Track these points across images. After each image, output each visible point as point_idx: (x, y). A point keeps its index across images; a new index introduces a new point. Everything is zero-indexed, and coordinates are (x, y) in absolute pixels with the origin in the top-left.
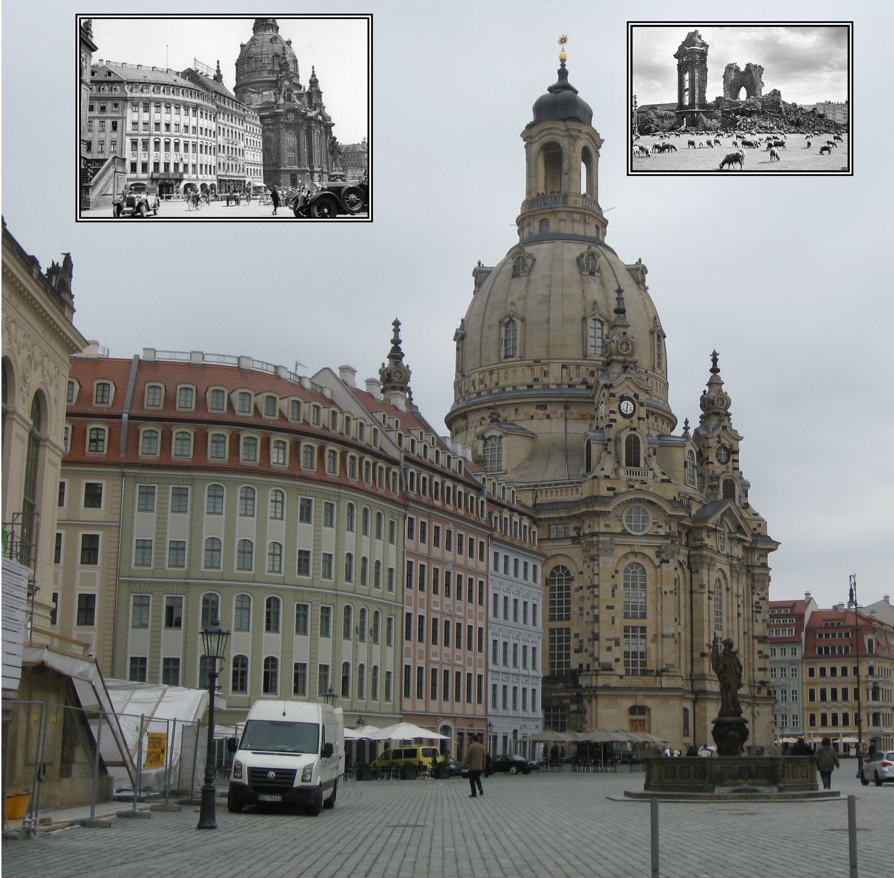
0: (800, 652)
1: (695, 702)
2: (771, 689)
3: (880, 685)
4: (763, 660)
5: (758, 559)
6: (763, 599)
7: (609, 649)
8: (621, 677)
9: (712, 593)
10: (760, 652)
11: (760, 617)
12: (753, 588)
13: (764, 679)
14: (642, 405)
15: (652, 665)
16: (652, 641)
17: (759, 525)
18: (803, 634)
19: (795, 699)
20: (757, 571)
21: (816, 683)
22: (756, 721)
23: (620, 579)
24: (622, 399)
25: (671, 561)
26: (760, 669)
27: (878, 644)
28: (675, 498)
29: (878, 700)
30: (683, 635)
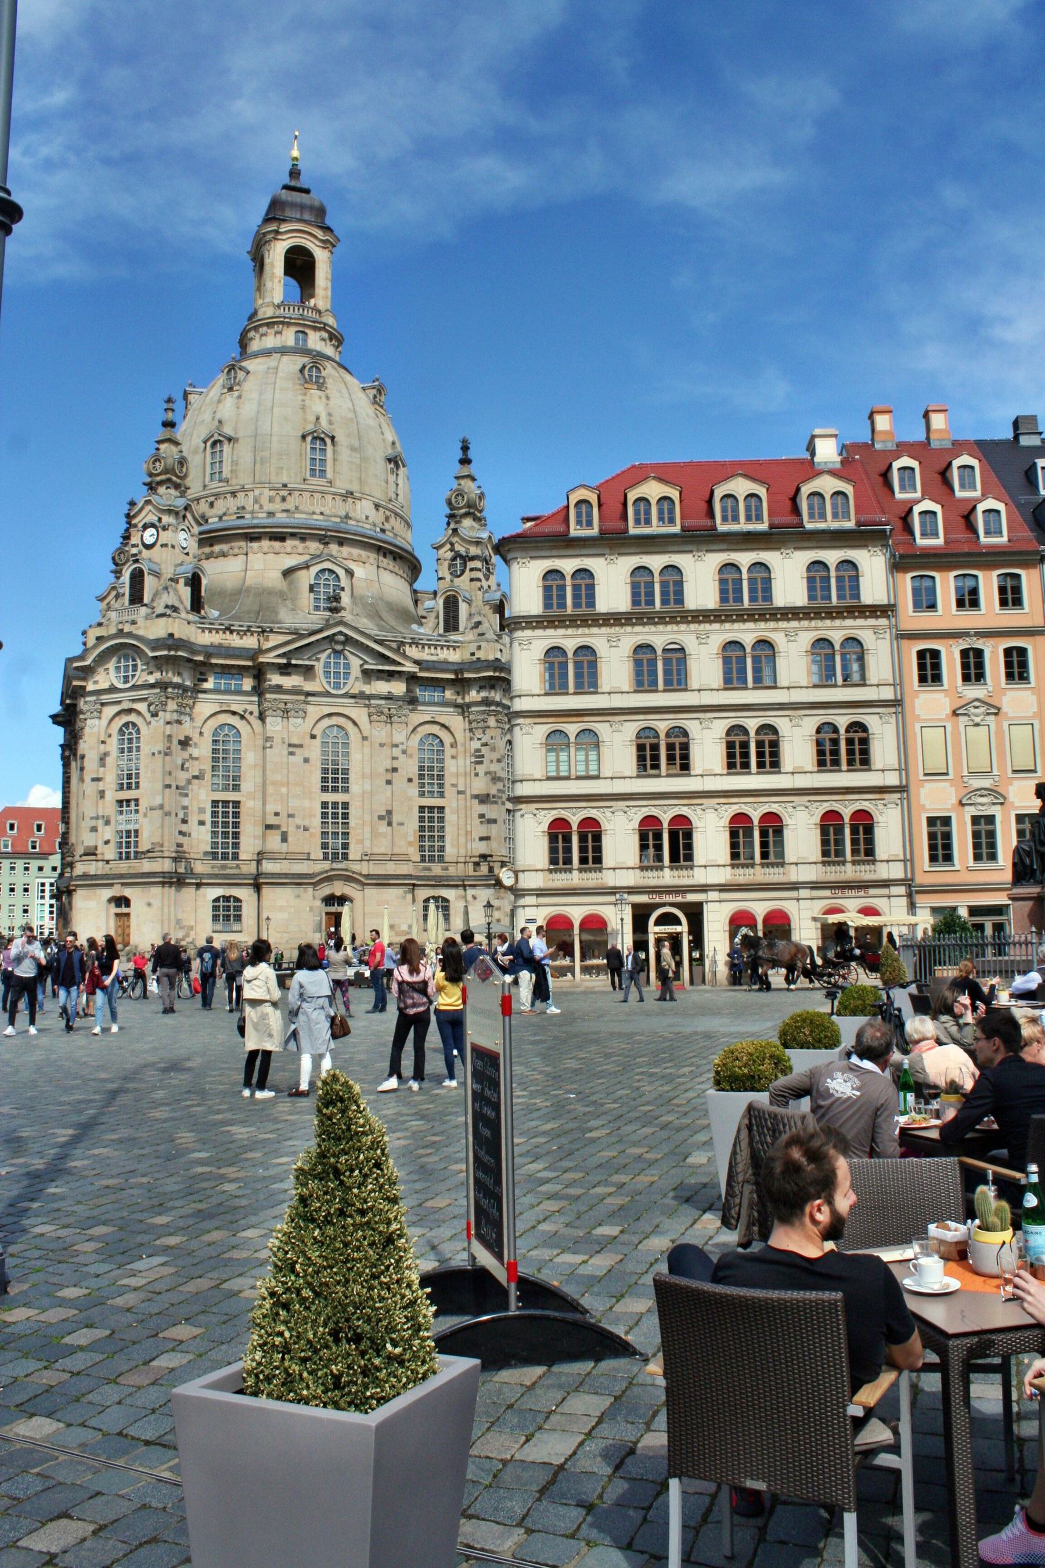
1: (257, 887)
4: (485, 826)
7: (94, 829)
8: (108, 862)
9: (301, 746)
10: (482, 816)
11: (481, 769)
12: (471, 730)
14: (164, 529)
15: (144, 846)
16: (145, 815)
17: (479, 648)
20: (473, 709)
23: (113, 746)
24: (145, 527)
25: (161, 714)
26: (481, 839)
28: (171, 635)
30: (250, 806)
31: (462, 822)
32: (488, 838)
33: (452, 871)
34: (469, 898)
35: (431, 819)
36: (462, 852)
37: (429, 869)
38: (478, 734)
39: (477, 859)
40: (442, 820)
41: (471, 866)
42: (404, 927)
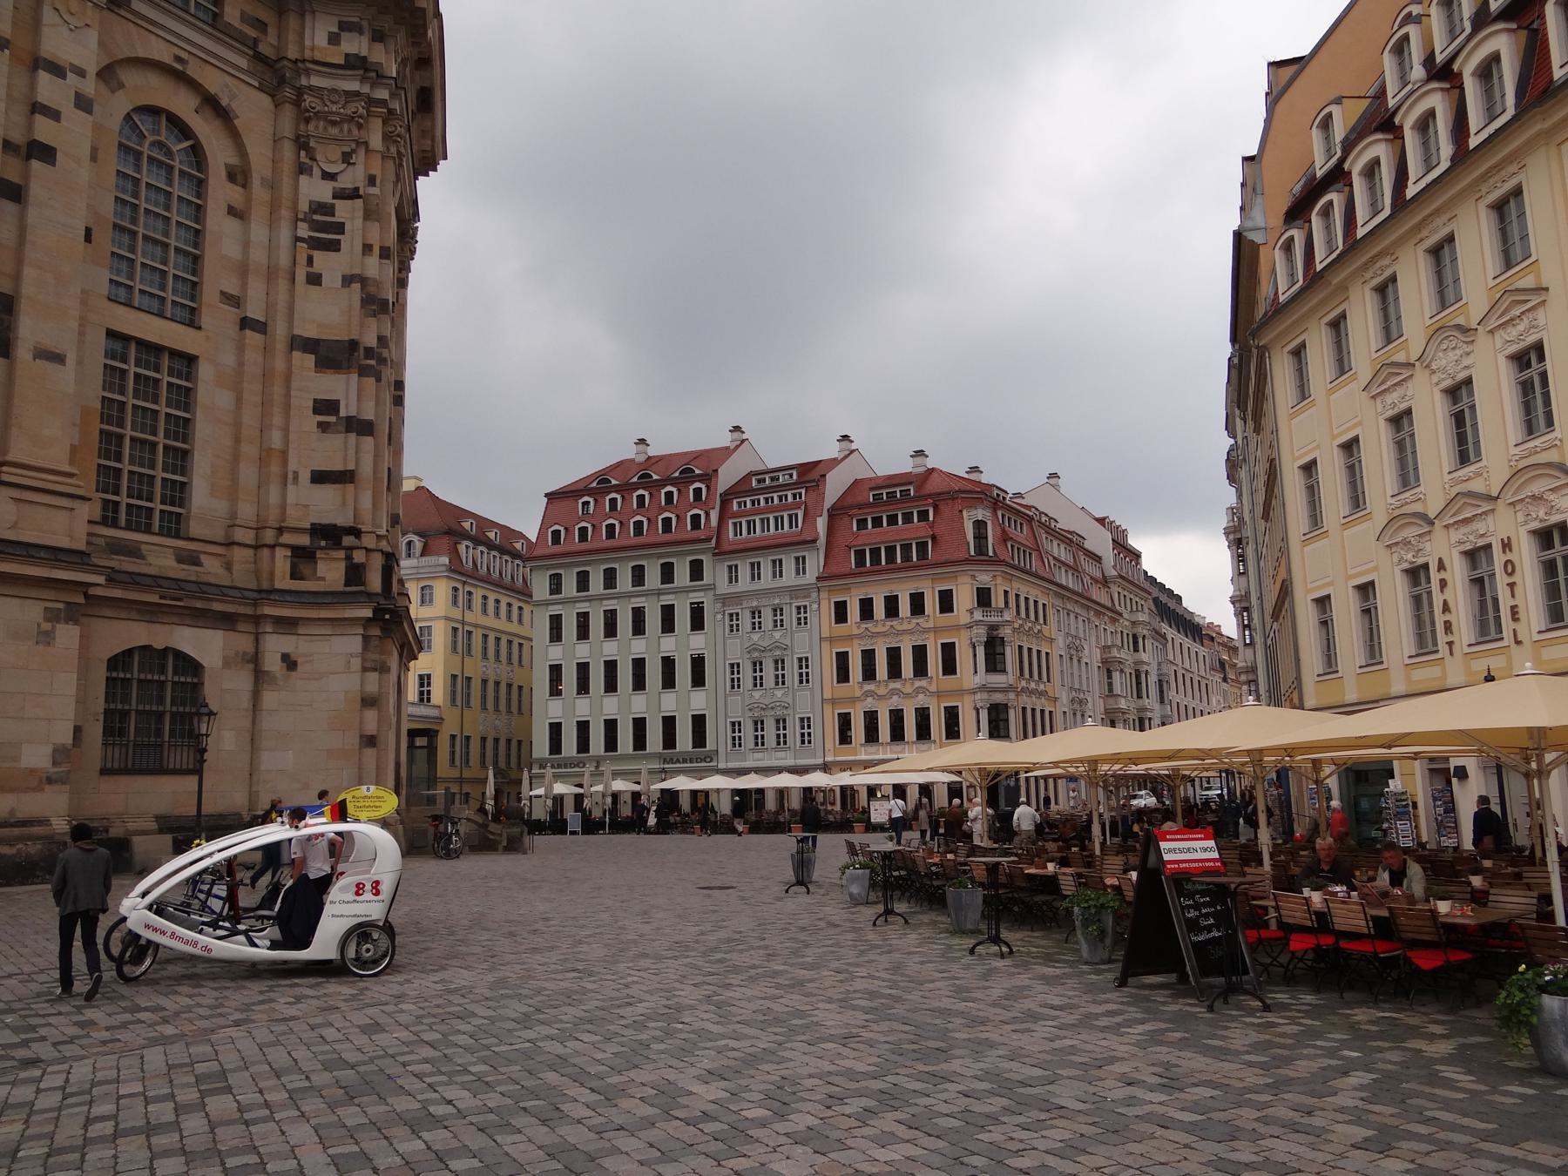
0: (815, 563)
2: (359, 557)
3: (1006, 632)
5: (334, 39)
6: (353, 194)
10: (326, 407)
11: (330, 266)
12: (301, 143)
13: (343, 519)
18: (821, 524)
19: (804, 679)
21: (851, 637)
22: (270, 698)
26: (320, 477)
27: (1005, 538)
29: (1004, 671)
31: (250, 417)
32: (344, 477)
33: (212, 568)
34: (272, 663)
35: (147, 387)
36: (247, 511)
37: (134, 551)
38: (328, 158)
39: (305, 540)
40: (184, 397)
41: (282, 556)
42: (37, 757)
